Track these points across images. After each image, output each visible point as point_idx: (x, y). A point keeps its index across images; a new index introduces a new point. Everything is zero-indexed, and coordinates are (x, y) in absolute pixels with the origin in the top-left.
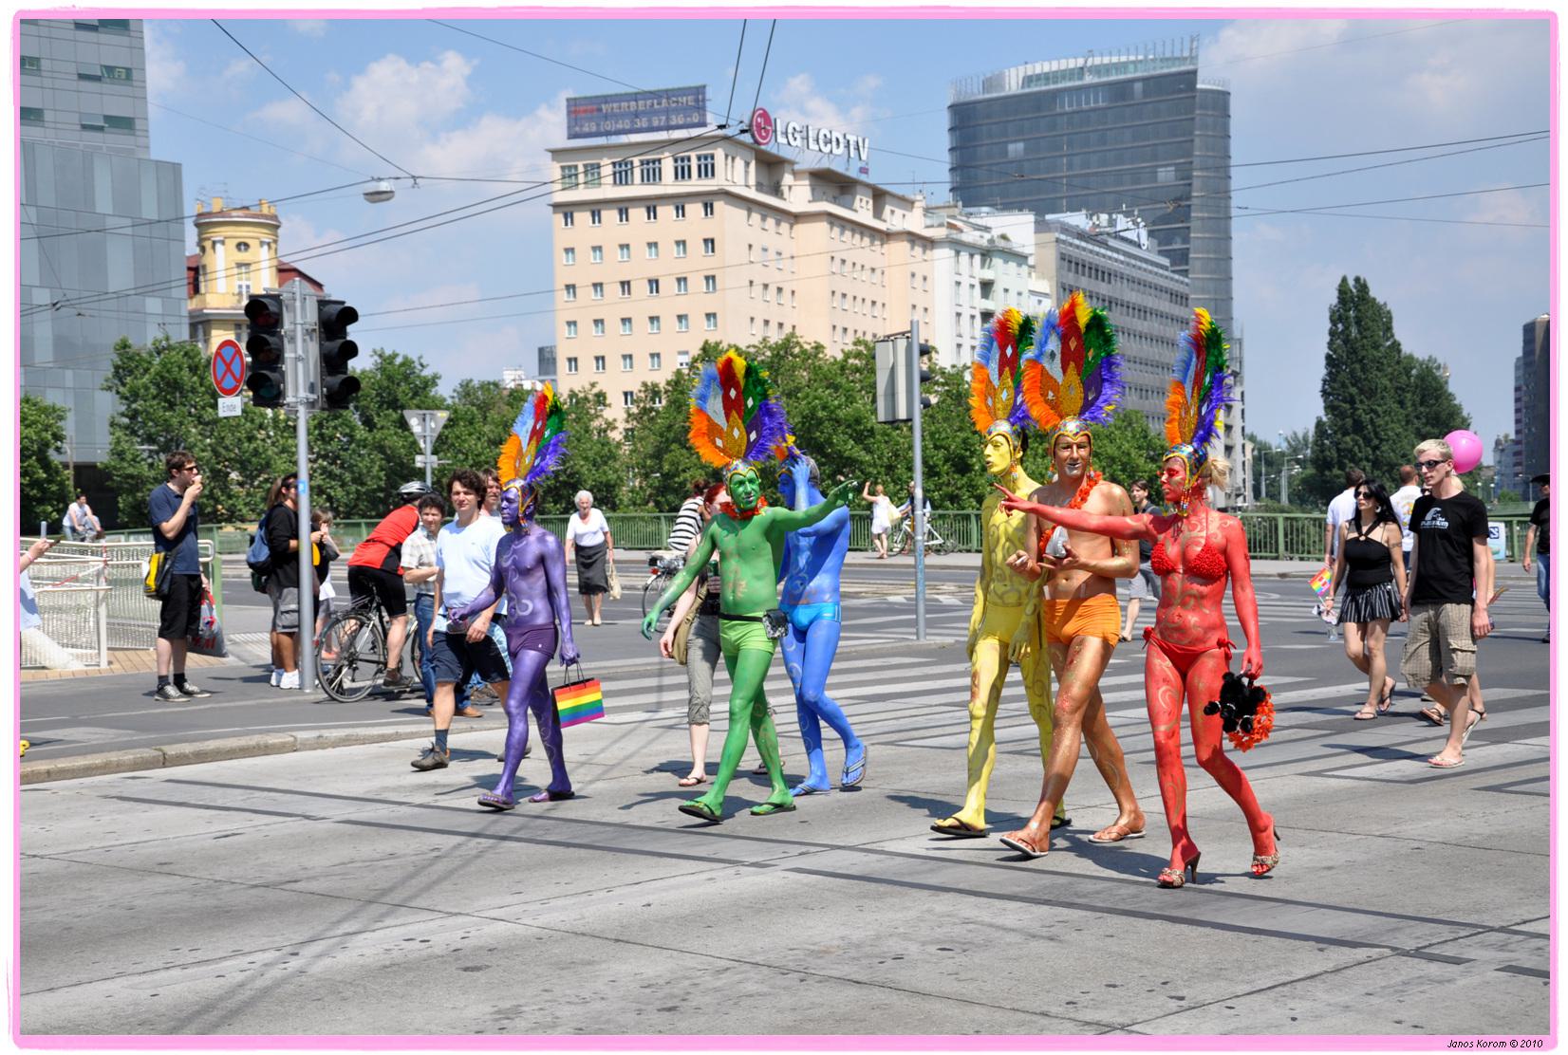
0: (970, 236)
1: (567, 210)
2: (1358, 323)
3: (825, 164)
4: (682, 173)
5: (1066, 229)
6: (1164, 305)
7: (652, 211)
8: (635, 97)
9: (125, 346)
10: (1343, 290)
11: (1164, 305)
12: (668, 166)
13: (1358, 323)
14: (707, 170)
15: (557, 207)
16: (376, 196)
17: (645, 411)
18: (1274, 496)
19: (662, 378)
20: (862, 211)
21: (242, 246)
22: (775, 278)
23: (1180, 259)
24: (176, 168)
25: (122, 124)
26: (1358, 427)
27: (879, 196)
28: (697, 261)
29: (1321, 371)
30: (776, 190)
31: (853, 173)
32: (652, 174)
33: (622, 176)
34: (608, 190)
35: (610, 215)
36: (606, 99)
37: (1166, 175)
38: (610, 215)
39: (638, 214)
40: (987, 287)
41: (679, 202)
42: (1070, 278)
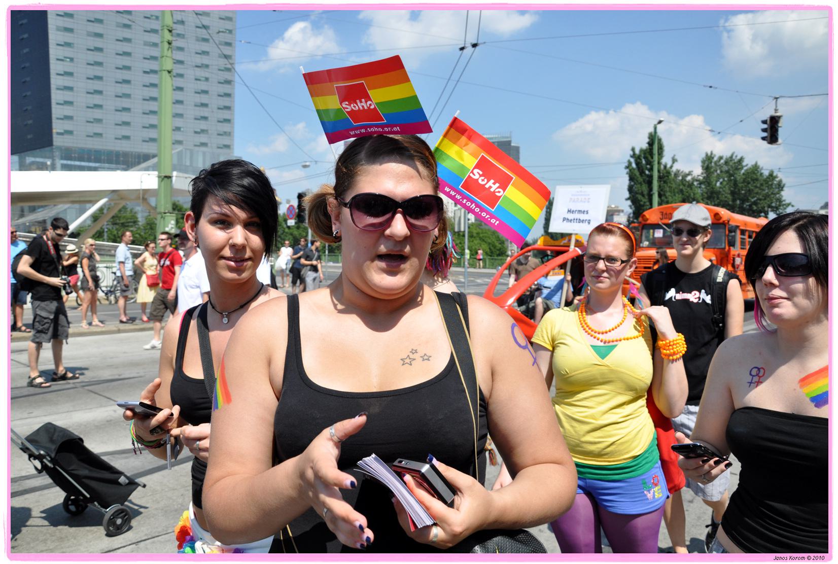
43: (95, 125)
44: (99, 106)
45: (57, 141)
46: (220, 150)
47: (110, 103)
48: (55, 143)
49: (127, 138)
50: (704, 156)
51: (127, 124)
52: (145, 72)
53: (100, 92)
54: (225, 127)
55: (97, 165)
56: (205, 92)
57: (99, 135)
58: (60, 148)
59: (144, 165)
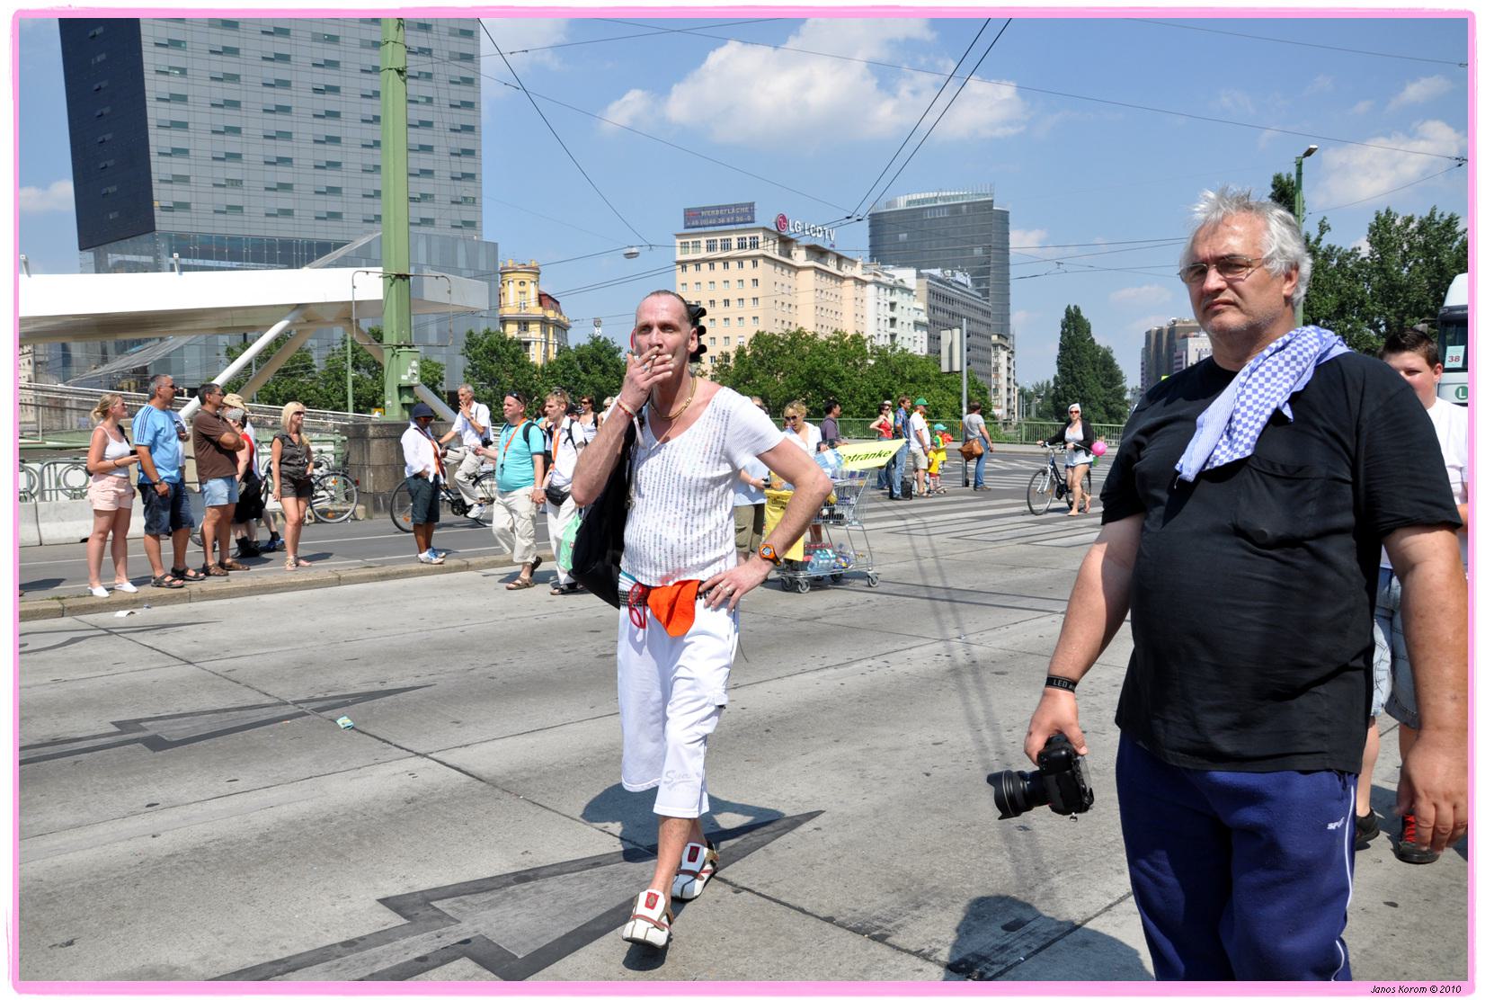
0: (884, 279)
1: (684, 264)
2: (1074, 326)
3: (813, 243)
4: (742, 246)
5: (931, 277)
6: (979, 317)
7: (726, 265)
8: (719, 208)
9: (470, 334)
10: (1068, 311)
11: (979, 317)
12: (735, 244)
13: (1074, 326)
14: (755, 245)
15: (678, 263)
16: (630, 256)
17: (722, 366)
18: (1028, 413)
19: (731, 350)
20: (831, 266)
21: (523, 283)
22: (788, 300)
23: (986, 293)
24: (495, 245)
25: (470, 224)
26: (1074, 380)
27: (840, 258)
28: (749, 291)
29: (1057, 352)
30: (789, 255)
31: (827, 247)
32: (726, 246)
33: (711, 248)
34: (704, 254)
35: (705, 266)
36: (704, 209)
37: (978, 251)
38: (705, 266)
39: (719, 265)
40: (893, 305)
41: (740, 260)
42: (934, 302)
43: (228, 190)
44: (236, 157)
45: (163, 221)
46: (457, 232)
47: (256, 150)
48: (157, 227)
49: (287, 213)
50: (1373, 220)
51: (285, 187)
52: (316, 90)
53: (236, 131)
54: (465, 188)
55: (235, 264)
56: (428, 124)
57: (240, 208)
58: (168, 236)
59: (318, 262)
